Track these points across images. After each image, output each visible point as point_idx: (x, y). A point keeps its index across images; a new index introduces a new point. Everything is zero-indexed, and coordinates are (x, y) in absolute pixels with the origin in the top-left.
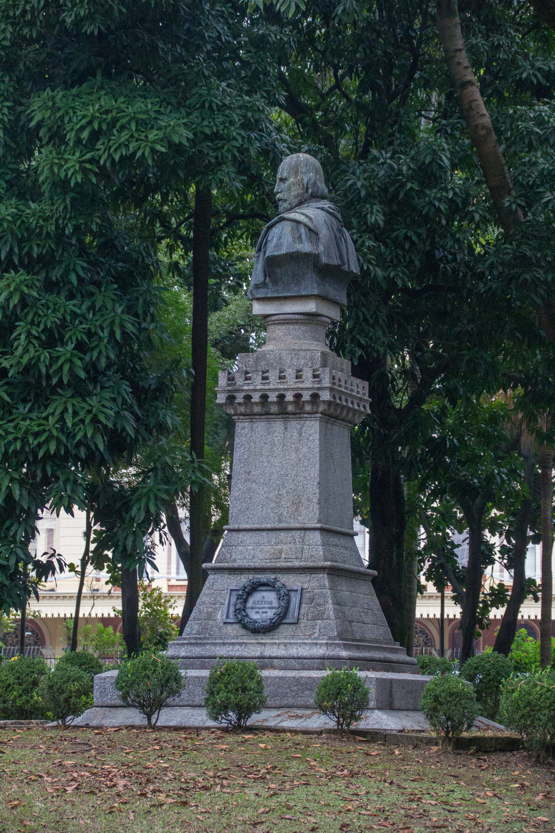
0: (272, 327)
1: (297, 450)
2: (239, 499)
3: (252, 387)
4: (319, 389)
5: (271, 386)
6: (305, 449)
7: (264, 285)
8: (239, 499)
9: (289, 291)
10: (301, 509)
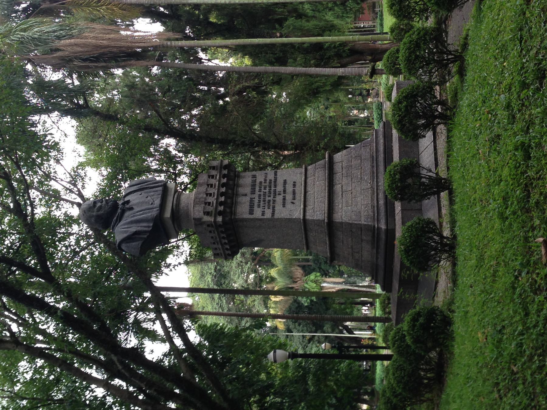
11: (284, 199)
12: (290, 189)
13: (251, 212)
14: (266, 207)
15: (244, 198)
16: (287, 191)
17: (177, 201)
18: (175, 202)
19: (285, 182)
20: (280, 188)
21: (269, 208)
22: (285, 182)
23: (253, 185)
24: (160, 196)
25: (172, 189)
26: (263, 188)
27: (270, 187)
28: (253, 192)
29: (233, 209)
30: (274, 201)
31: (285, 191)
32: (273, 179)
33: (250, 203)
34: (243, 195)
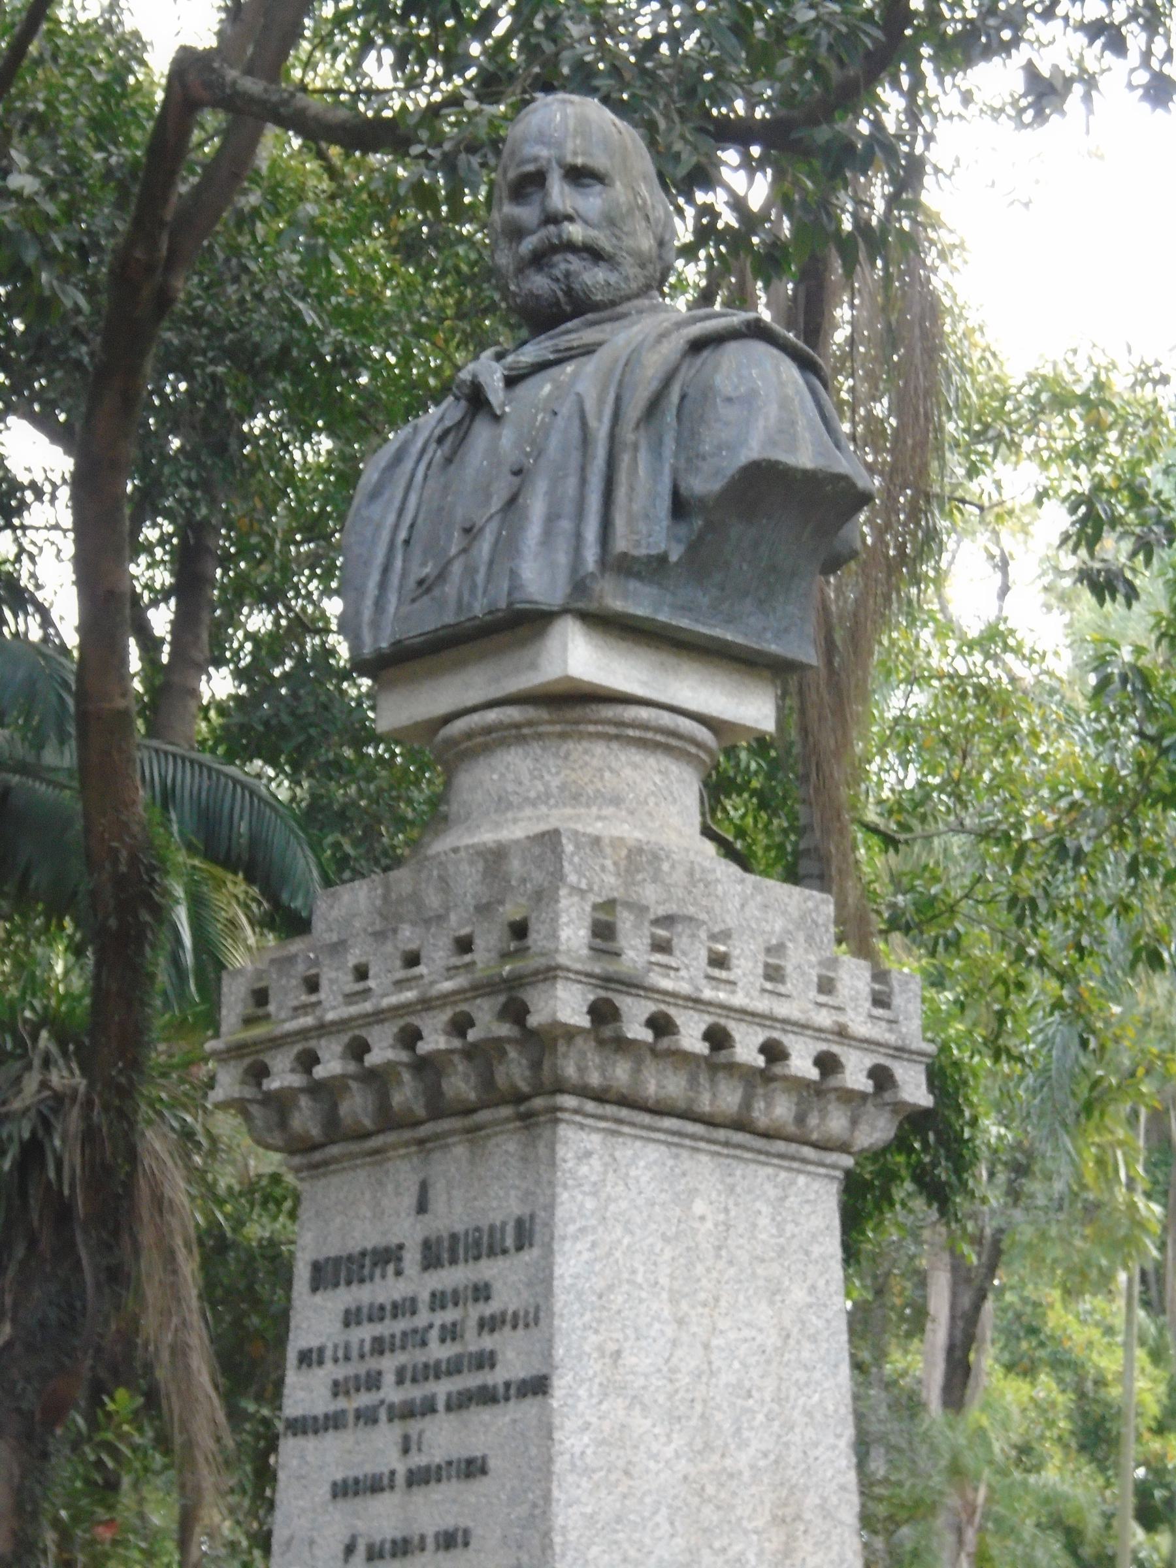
0: (599, 748)
1: (775, 1291)
2: (588, 1471)
3: (685, 988)
4: (901, 1051)
5: (738, 1000)
6: (799, 1295)
7: (653, 569)
8: (588, 1471)
9: (730, 620)
10: (805, 1546)
11: (375, 1486)
12: (433, 1510)
13: (325, 1275)
14: (341, 1372)
15: (409, 1200)
16: (419, 1495)
17: (469, 735)
18: (460, 725)
19: (474, 1468)
20: (443, 1438)
21: (338, 1389)
22: (474, 1468)
23: (484, 1244)
24: (449, 618)
25: (533, 666)
26: (449, 1315)
27: (454, 1368)
28: (434, 1255)
29: (335, 1150)
30: (367, 1417)
31: (419, 1478)
32: (496, 1377)
33: (375, 1251)
34: (424, 1188)
